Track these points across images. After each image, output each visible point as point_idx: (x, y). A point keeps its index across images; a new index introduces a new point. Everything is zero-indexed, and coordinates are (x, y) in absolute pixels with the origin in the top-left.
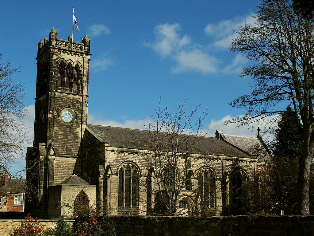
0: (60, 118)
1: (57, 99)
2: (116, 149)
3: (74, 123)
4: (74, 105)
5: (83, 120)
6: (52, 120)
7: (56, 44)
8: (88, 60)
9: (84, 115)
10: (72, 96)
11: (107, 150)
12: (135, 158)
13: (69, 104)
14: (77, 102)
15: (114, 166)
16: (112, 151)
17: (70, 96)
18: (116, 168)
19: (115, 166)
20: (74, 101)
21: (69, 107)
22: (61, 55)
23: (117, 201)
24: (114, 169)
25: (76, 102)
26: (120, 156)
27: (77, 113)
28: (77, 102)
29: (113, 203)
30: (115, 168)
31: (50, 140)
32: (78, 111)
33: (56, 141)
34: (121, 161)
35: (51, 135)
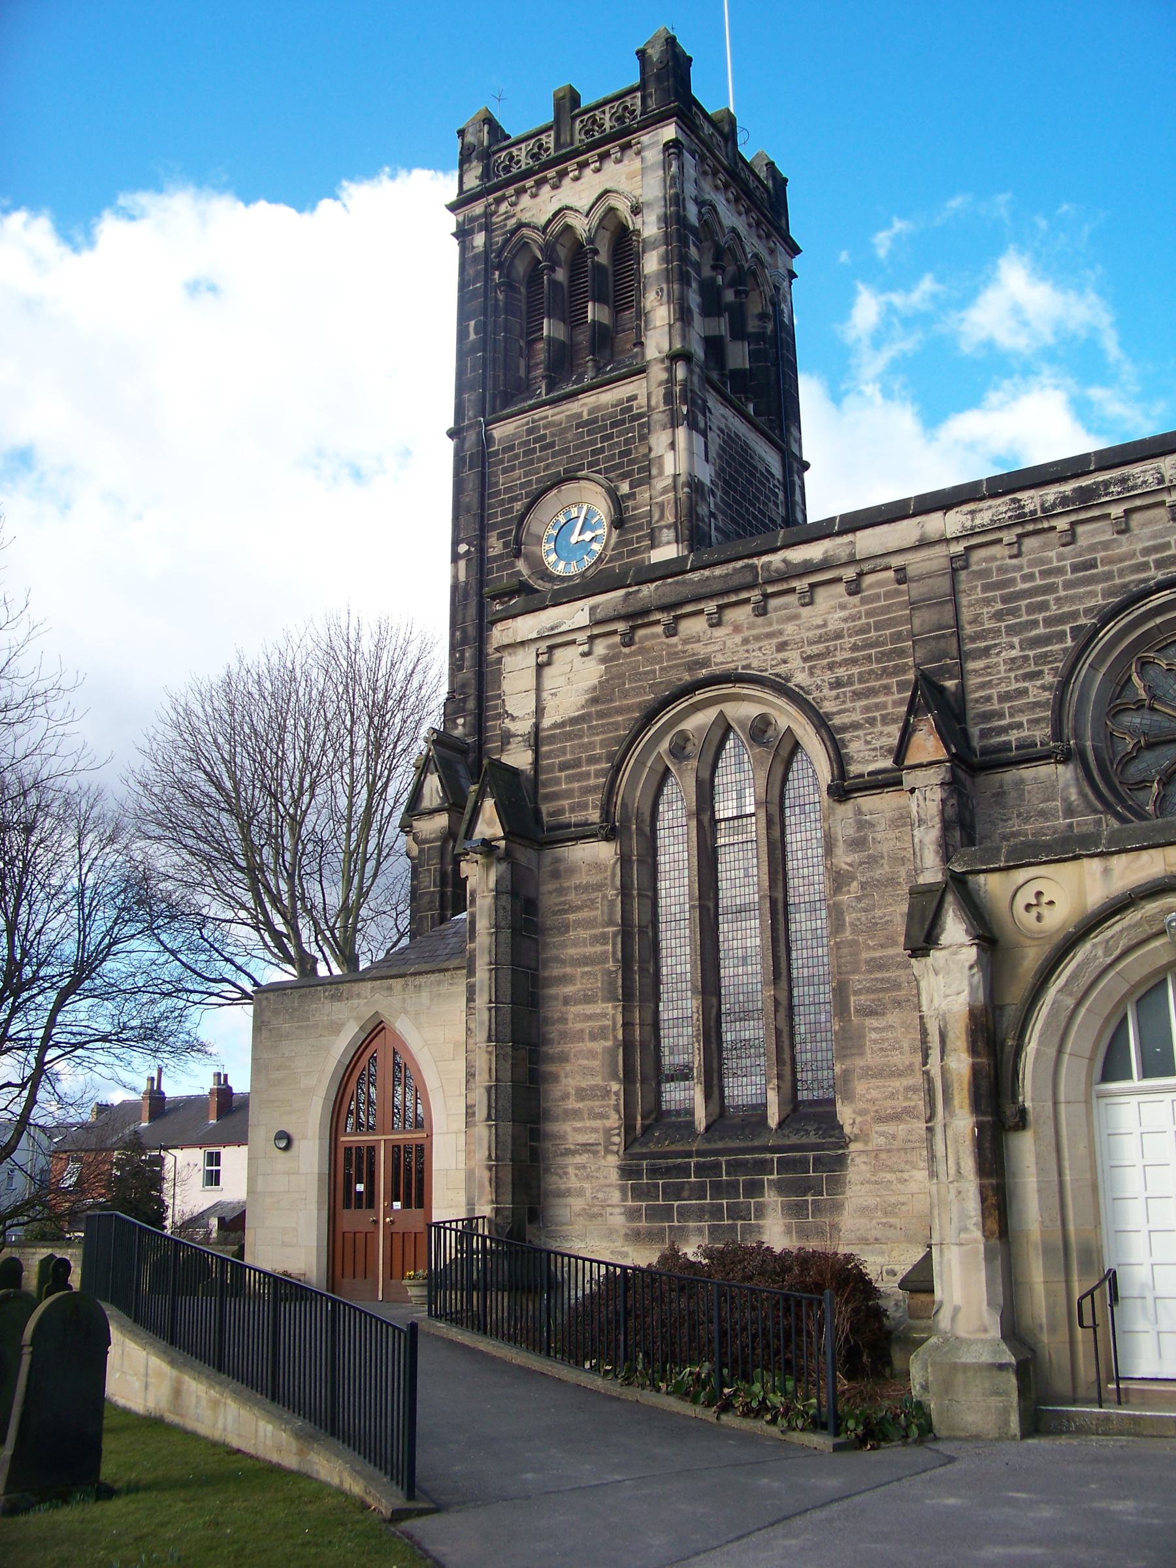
0: (521, 565)
1: (502, 461)
2: (576, 614)
3: (607, 562)
4: (602, 450)
5: (656, 517)
7: (485, 175)
8: (667, 146)
9: (660, 484)
10: (583, 405)
12: (769, 636)
13: (571, 459)
14: (623, 422)
15: (577, 763)
17: (573, 407)
18: (598, 774)
19: (592, 760)
20: (604, 428)
21: (570, 477)
22: (514, 216)
23: (614, 1076)
24: (587, 791)
25: (614, 425)
27: (625, 488)
28: (623, 422)
29: (582, 1094)
30: (587, 775)
31: (460, 721)
32: (624, 476)
35: (463, 686)
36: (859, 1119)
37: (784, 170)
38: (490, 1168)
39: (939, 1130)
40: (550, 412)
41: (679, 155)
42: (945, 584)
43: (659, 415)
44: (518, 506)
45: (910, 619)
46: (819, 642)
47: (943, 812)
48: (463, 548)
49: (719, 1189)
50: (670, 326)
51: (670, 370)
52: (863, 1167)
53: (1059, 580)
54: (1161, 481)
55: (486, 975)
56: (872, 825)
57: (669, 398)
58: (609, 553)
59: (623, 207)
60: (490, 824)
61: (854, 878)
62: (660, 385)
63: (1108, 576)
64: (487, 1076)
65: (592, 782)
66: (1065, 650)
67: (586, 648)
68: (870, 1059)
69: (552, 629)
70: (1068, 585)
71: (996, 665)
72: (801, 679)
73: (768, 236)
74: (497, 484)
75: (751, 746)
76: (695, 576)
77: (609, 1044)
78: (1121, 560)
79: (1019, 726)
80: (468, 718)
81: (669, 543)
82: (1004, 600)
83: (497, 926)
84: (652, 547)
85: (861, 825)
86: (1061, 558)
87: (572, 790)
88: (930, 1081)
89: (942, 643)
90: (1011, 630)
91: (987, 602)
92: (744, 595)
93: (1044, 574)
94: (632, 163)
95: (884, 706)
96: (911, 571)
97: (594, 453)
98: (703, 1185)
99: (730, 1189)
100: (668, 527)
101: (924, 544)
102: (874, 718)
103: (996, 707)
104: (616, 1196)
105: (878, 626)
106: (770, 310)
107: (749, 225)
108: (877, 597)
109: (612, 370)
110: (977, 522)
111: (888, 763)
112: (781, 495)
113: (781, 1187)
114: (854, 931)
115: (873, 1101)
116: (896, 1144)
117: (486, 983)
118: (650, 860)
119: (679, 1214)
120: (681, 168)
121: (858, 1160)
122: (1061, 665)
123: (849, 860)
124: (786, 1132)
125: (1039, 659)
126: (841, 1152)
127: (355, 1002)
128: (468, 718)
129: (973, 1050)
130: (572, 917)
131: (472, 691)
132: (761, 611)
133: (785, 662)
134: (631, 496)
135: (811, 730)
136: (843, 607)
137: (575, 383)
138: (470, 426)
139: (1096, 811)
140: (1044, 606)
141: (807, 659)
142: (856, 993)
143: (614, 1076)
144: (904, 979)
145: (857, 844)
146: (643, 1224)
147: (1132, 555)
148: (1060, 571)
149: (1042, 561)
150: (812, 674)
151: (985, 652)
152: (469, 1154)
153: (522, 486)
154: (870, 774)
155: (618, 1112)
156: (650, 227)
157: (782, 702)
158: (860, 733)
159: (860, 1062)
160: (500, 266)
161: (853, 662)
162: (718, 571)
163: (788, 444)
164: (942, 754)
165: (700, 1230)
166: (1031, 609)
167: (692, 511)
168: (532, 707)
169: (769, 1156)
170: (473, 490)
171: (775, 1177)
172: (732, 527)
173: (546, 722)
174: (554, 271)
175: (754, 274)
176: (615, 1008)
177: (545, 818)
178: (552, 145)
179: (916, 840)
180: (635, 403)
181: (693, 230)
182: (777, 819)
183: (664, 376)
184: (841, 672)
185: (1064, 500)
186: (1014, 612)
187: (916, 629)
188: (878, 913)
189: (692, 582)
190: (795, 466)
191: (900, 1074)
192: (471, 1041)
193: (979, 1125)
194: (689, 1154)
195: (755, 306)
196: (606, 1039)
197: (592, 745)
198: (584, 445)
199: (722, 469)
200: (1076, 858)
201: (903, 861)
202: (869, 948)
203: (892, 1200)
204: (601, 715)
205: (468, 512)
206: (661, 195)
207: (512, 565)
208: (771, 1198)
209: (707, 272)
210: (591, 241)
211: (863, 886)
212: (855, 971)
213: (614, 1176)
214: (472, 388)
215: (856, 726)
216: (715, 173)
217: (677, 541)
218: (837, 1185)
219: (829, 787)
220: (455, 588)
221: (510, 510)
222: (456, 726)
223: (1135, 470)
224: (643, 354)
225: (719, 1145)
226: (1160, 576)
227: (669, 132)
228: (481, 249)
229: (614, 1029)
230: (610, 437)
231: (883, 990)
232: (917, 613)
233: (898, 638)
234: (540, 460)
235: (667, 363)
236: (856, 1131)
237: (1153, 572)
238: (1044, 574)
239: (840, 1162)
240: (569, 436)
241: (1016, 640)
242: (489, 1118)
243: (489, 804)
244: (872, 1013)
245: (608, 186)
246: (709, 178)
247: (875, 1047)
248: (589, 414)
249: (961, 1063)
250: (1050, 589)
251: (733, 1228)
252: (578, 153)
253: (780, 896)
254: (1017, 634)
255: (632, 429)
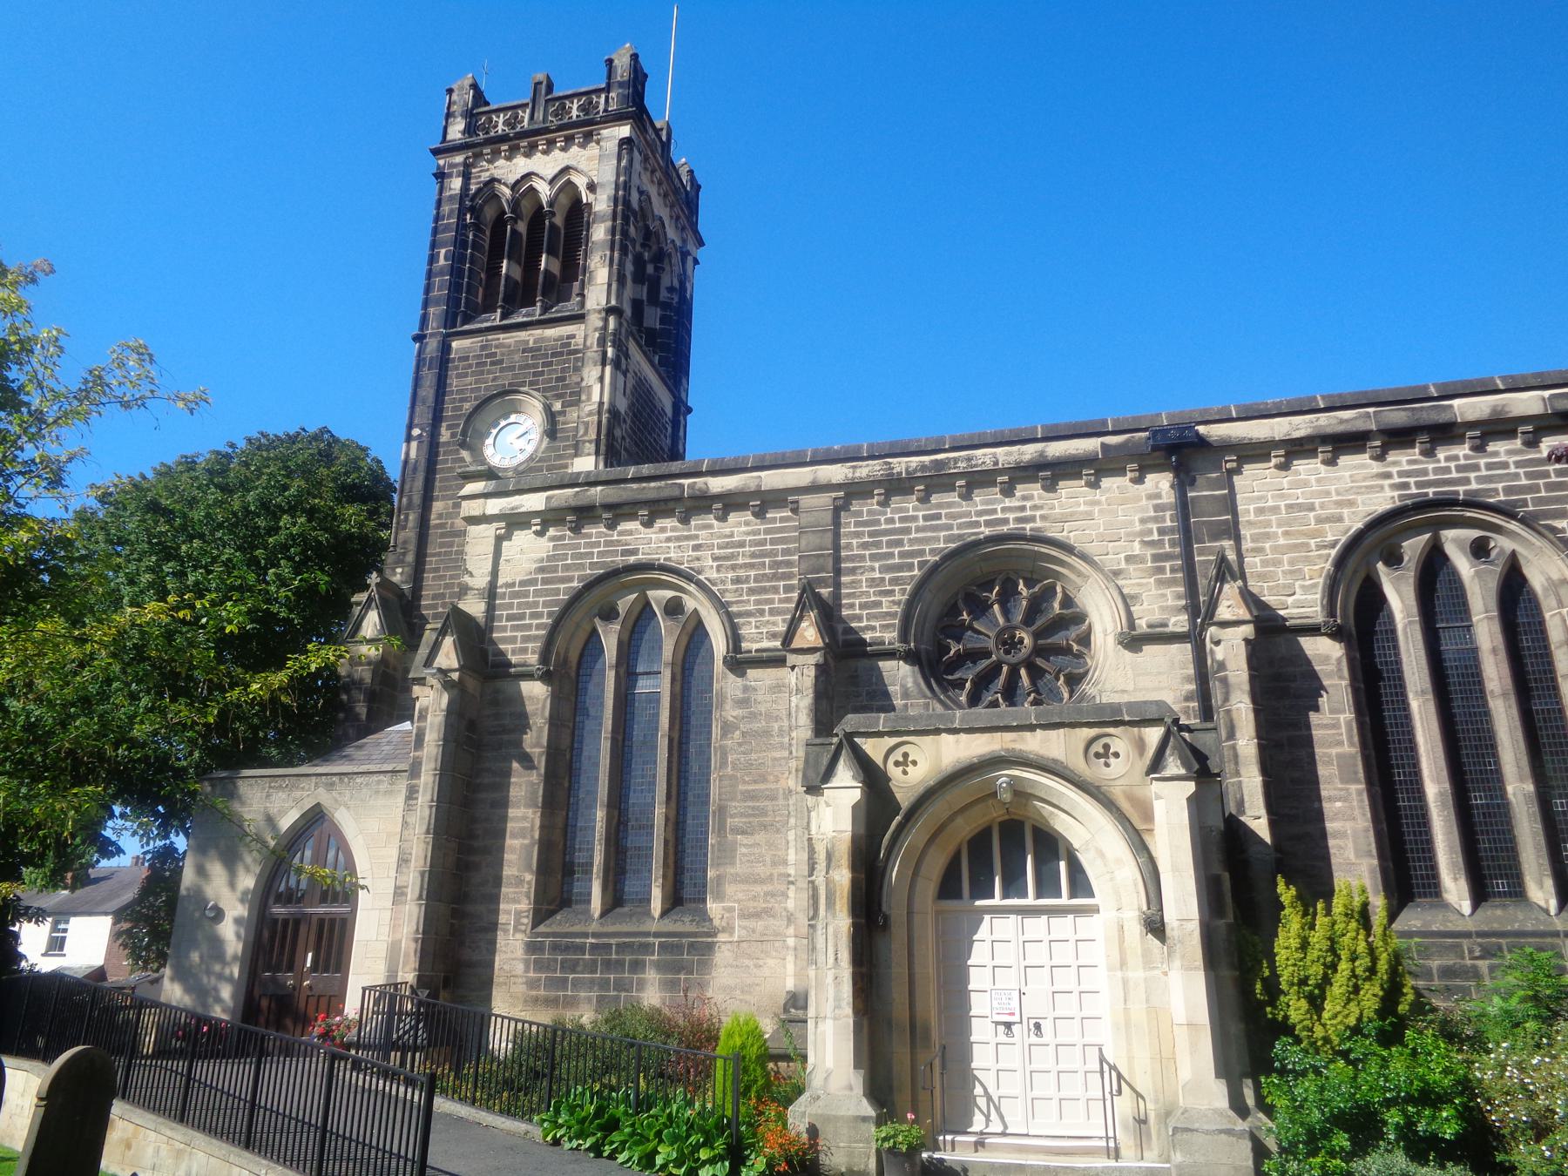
0: (465, 454)
1: (457, 368)
2: (534, 502)
5: (581, 432)
6: (415, 469)
10: (530, 336)
11: (473, 520)
14: (561, 354)
15: (522, 617)
16: (515, 522)
17: (522, 335)
19: (535, 615)
23: (529, 868)
24: (526, 639)
25: (553, 355)
26: (578, 546)
27: (557, 406)
28: (561, 354)
30: (529, 627)
31: (399, 570)
32: (558, 397)
33: (436, 570)
34: (580, 579)
36: (726, 915)
37: (700, 180)
38: (416, 940)
39: (819, 926)
40: (502, 336)
41: (630, 152)
42: (828, 517)
43: (593, 353)
44: (468, 407)
45: (798, 539)
46: (726, 548)
47: (816, 685)
48: (416, 432)
49: (608, 965)
50: (609, 285)
51: (606, 321)
52: (727, 954)
53: (913, 525)
54: (996, 463)
55: (431, 779)
56: (755, 690)
57: (602, 342)
58: (540, 455)
59: (580, 182)
60: (447, 655)
61: (738, 728)
62: (596, 330)
63: (950, 527)
64: (422, 862)
65: (534, 632)
66: (912, 577)
67: (539, 528)
68: (739, 868)
69: (513, 509)
70: (918, 530)
71: (861, 581)
72: (710, 573)
73: (683, 229)
74: (451, 384)
75: (664, 620)
76: (635, 486)
77: (527, 842)
78: (961, 517)
79: (873, 628)
80: (406, 569)
81: (589, 454)
82: (871, 534)
83: (445, 739)
84: (576, 455)
85: (746, 689)
86: (915, 509)
87: (516, 637)
88: (815, 889)
89: (821, 560)
90: (873, 557)
91: (858, 535)
92: (671, 505)
93: (902, 520)
94: (593, 150)
95: (771, 601)
96: (801, 502)
97: (535, 374)
98: (594, 962)
99: (620, 964)
100: (590, 442)
101: (815, 488)
102: (764, 610)
103: (858, 612)
104: (520, 968)
105: (773, 542)
106: (676, 284)
107: (671, 217)
108: (774, 520)
109: (556, 312)
110: (857, 475)
111: (777, 644)
112: (669, 429)
113: (661, 967)
114: (733, 768)
115: (739, 901)
116: (756, 937)
117: (430, 785)
118: (573, 699)
119: (573, 984)
120: (631, 161)
121: (723, 947)
122: (909, 587)
123: (734, 714)
124: (666, 921)
125: (894, 581)
126: (710, 940)
127: (298, 794)
128: (406, 569)
129: (854, 868)
130: (506, 737)
131: (412, 547)
132: (685, 521)
133: (698, 559)
134: (563, 413)
135: (713, 612)
136: (747, 523)
137: (527, 315)
138: (432, 335)
139: (925, 697)
140: (899, 543)
141: (715, 559)
142: (731, 816)
143: (529, 868)
144: (770, 808)
145: (743, 703)
146: (542, 992)
147: (969, 514)
148: (915, 518)
149: (901, 510)
150: (719, 569)
151: (853, 571)
152: (394, 927)
153: (472, 390)
154: (757, 651)
155: (529, 898)
156: (601, 203)
157: (692, 588)
158: (752, 620)
159: (730, 870)
160: (472, 210)
161: (752, 566)
162: (653, 484)
163: (679, 391)
164: (821, 644)
165: (589, 1000)
166: (890, 544)
167: (610, 433)
168: (488, 566)
169: (651, 940)
170: (430, 387)
171: (655, 957)
172: (635, 449)
173: (501, 582)
174: (515, 220)
175: (670, 255)
176: (535, 813)
177: (490, 658)
178: (526, 120)
179: (793, 704)
180: (573, 341)
181: (635, 213)
182: (679, 677)
183: (600, 324)
184: (742, 573)
185: (923, 467)
186: (878, 545)
187: (802, 548)
188: (754, 756)
189: (632, 489)
190: (681, 409)
191: (762, 882)
192: (405, 832)
193: (854, 925)
194: (586, 935)
195: (666, 281)
196: (524, 838)
197: (536, 604)
198: (528, 366)
199: (633, 404)
200: (937, 732)
201: (777, 718)
202: (745, 782)
203: (749, 981)
204: (545, 581)
205: (424, 403)
206: (613, 179)
207: (457, 452)
208: (652, 975)
209: (638, 248)
210: (551, 204)
211: (744, 734)
212: (732, 800)
213: (519, 952)
214: (437, 304)
215: (749, 614)
216: (653, 172)
217: (597, 453)
218: (705, 966)
219: (725, 658)
220: (406, 462)
221: (460, 408)
222: (395, 574)
223: (979, 452)
224: (582, 304)
225: (611, 929)
226: (987, 531)
227: (625, 131)
228: (458, 192)
229: (532, 826)
230: (551, 364)
231: (753, 815)
232: (804, 536)
233: (786, 552)
234: (489, 372)
235: (603, 314)
236: (724, 924)
237: (982, 529)
238: (902, 520)
239: (709, 948)
240: (517, 357)
241: (877, 565)
242: (420, 898)
243: (448, 642)
244: (743, 833)
245: (572, 163)
246: (648, 174)
247: (744, 859)
248: (535, 342)
249: (843, 877)
250: (907, 531)
251: (618, 997)
252: (547, 131)
253: (676, 736)
254: (878, 560)
255: (568, 361)
